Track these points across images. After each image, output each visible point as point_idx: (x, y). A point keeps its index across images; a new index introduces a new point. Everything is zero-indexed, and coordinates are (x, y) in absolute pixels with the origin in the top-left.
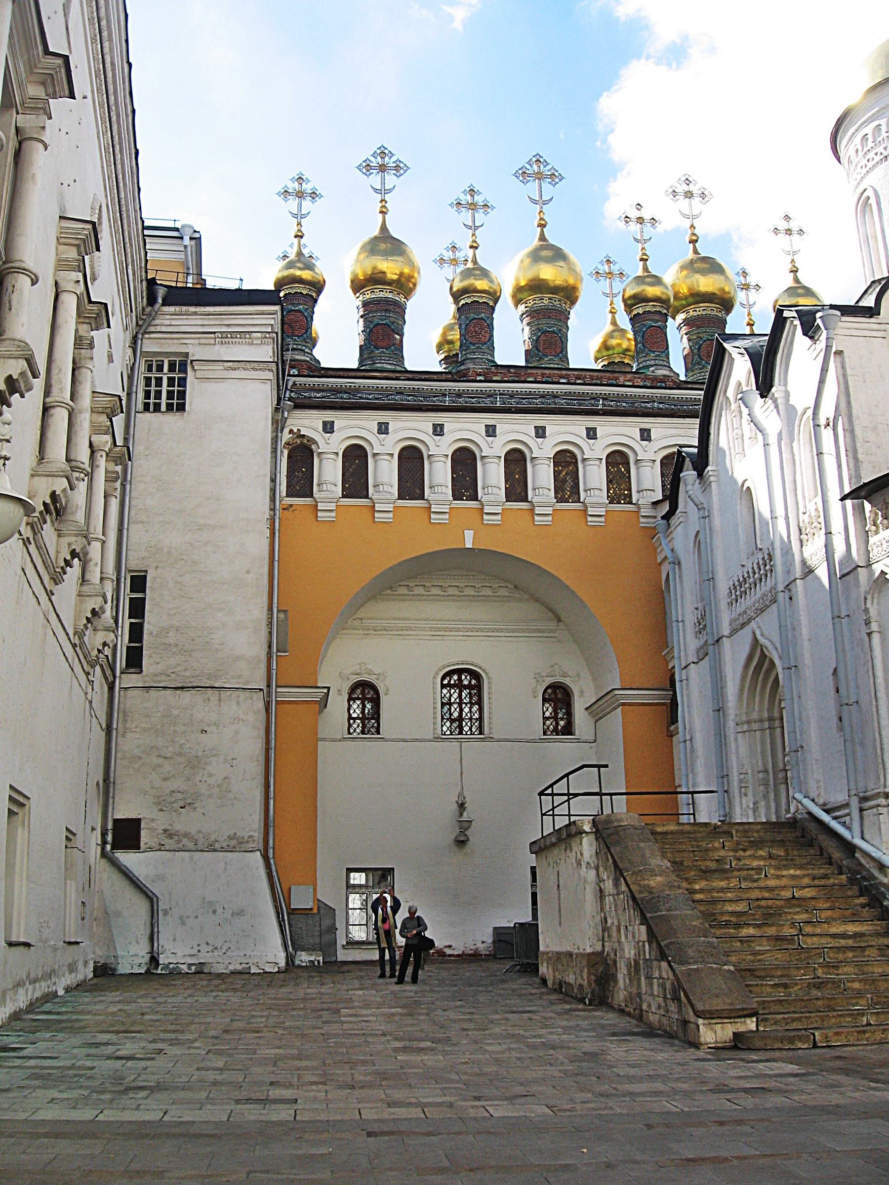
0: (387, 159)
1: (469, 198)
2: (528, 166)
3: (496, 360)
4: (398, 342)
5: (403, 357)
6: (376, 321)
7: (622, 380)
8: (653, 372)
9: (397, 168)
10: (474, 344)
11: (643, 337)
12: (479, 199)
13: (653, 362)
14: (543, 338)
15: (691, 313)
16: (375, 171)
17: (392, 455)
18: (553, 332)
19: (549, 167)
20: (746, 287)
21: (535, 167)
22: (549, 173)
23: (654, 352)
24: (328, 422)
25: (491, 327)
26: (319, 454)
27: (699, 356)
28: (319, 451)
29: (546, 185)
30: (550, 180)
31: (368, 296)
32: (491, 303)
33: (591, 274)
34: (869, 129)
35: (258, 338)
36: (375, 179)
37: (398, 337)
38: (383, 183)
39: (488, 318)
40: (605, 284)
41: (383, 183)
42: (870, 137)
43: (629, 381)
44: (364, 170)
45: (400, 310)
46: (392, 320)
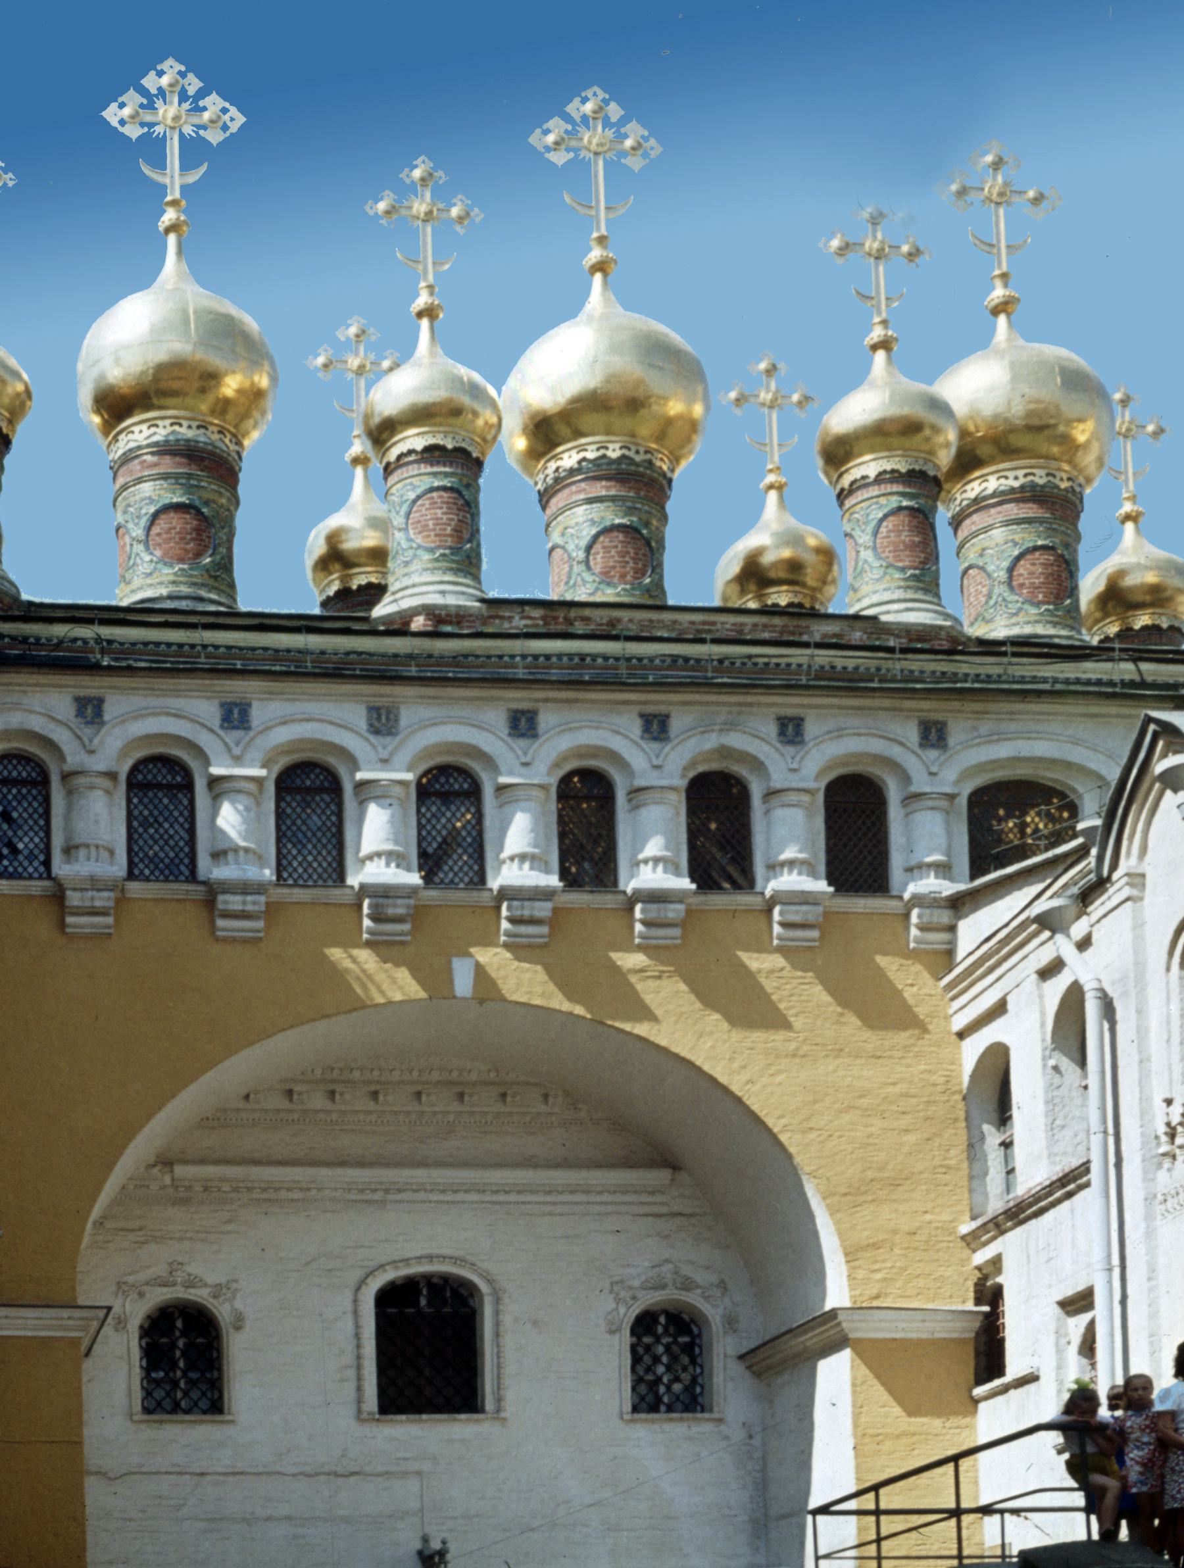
10: (431, 550)
23: (903, 570)
39: (468, 486)
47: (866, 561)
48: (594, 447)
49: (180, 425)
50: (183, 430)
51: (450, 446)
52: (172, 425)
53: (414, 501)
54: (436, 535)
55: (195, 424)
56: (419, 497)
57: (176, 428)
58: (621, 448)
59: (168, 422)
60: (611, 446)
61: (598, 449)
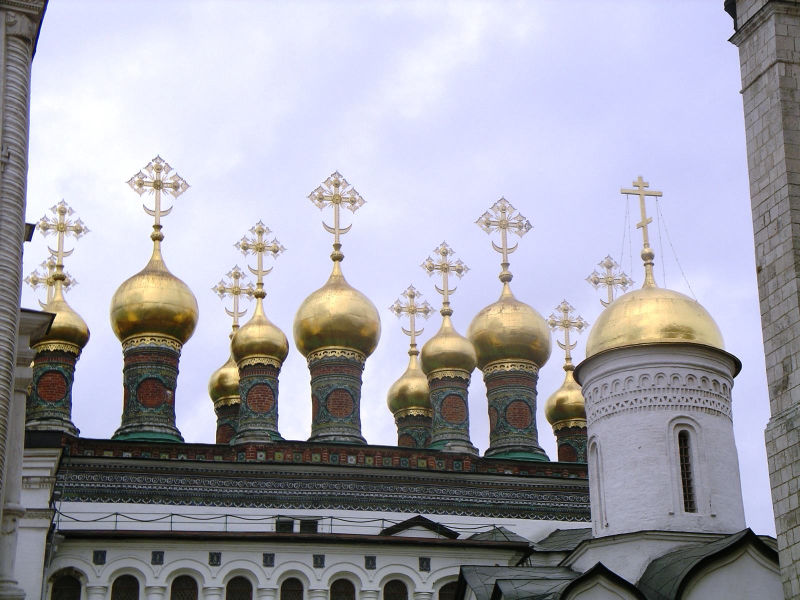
0: (163, 173)
1: (256, 236)
2: (325, 187)
3: (280, 430)
4: (170, 397)
5: (174, 416)
6: (146, 374)
7: (415, 458)
8: (450, 448)
9: (176, 187)
10: (255, 414)
11: (441, 406)
12: (267, 238)
13: (450, 436)
14: (332, 396)
15: (498, 369)
16: (149, 188)
17: (164, 588)
18: (345, 390)
19: (349, 189)
20: (567, 325)
21: (333, 187)
22: (349, 196)
23: (452, 424)
24: (100, 552)
25: (275, 392)
26: (88, 588)
27: (505, 418)
28: (88, 585)
29: (344, 210)
30: (349, 204)
31: (137, 345)
32: (275, 365)
33: (392, 308)
34: (598, 384)
35: (35, 483)
36: (149, 198)
37: (169, 392)
38: (158, 202)
40: (405, 320)
41: (158, 202)
42: (599, 391)
43: (423, 458)
44: (136, 187)
45: (174, 357)
46: (164, 373)
47: (437, 418)
48: (330, 351)
49: (155, 340)
50: (156, 342)
51: (266, 364)
52: (151, 340)
53: (250, 389)
54: (258, 406)
55: (161, 339)
56: (252, 387)
57: (153, 341)
58: (341, 352)
59: (149, 339)
60: (337, 351)
61: (332, 352)
